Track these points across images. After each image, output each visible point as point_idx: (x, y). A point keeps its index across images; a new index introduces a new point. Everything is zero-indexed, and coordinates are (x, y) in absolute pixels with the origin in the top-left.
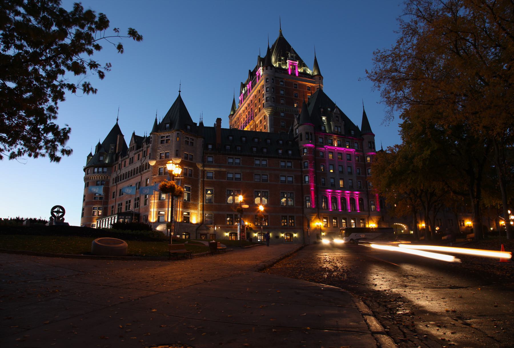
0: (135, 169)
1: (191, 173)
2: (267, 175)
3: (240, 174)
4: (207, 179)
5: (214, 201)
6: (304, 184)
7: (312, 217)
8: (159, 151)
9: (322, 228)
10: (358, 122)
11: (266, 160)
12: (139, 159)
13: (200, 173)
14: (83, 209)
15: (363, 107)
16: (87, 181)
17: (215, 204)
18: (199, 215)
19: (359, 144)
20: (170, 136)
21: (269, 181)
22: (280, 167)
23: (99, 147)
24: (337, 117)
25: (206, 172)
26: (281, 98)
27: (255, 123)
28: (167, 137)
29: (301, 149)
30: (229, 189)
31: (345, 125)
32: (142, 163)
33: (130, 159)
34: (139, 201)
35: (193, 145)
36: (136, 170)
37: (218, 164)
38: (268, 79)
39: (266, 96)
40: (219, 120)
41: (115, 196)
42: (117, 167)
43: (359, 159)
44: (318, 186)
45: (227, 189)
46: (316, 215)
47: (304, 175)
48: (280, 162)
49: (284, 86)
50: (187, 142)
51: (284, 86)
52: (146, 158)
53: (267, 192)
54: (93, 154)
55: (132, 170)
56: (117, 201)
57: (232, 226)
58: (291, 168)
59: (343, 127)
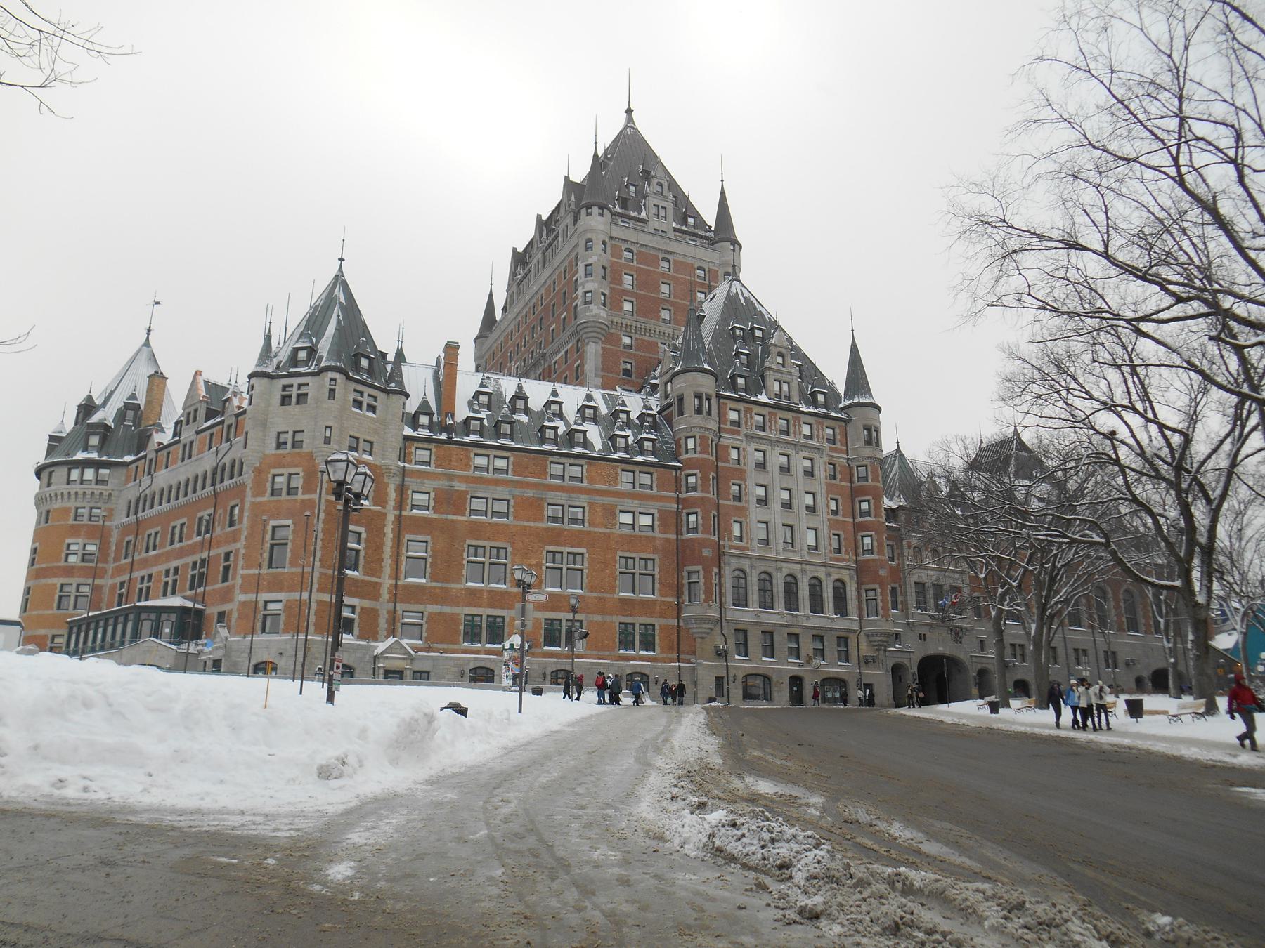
2: (583, 508)
10: (837, 375)
11: (582, 466)
14: (28, 591)
16: (47, 508)
19: (837, 431)
21: (586, 524)
24: (780, 354)
26: (624, 297)
28: (300, 386)
29: (680, 439)
33: (185, 446)
34: (205, 570)
43: (838, 473)
44: (722, 542)
45: (469, 542)
48: (619, 471)
53: (582, 554)
56: (136, 566)
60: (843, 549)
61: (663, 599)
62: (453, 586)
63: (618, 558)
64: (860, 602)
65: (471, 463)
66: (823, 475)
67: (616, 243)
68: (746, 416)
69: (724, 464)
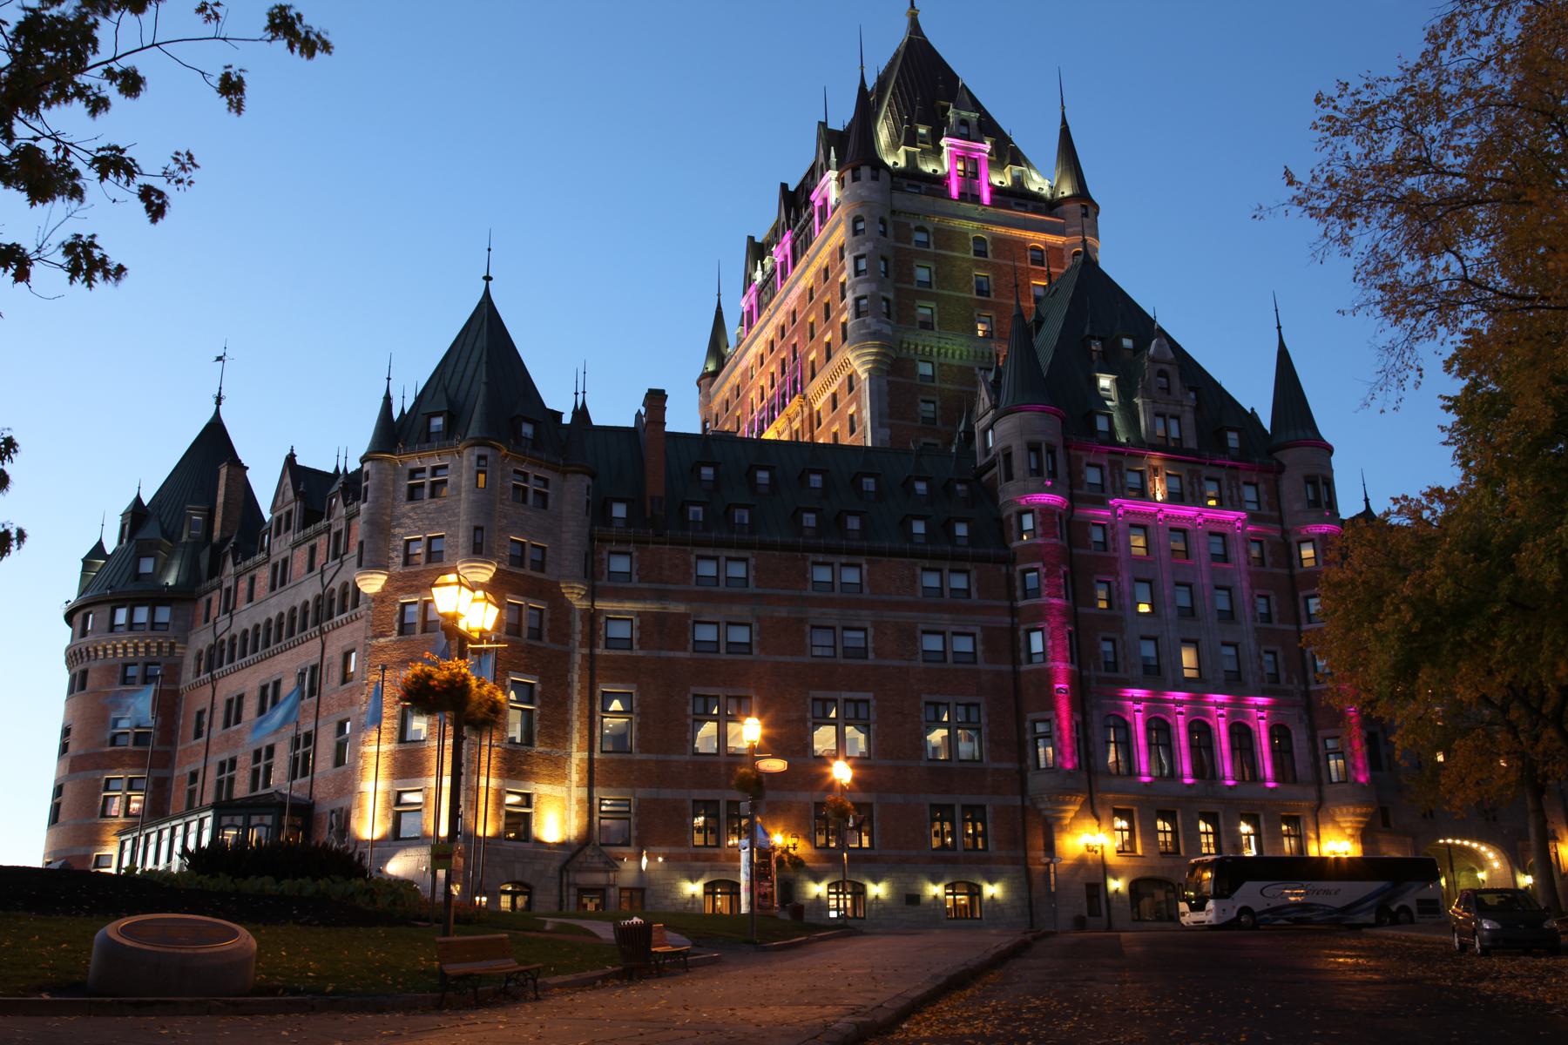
0: (294, 609)
1: (536, 625)
3: (750, 625)
4: (606, 647)
5: (638, 746)
6: (1025, 667)
7: (1065, 811)
8: (402, 531)
9: (1112, 858)
10: (1256, 396)
12: (311, 569)
13: (578, 626)
14: (58, 791)
15: (1279, 328)
16: (81, 667)
17: (644, 756)
18: (575, 807)
19: (1262, 487)
20: (445, 467)
21: (871, 655)
22: (920, 595)
23: (137, 515)
24: (1162, 373)
25: (602, 619)
27: (811, 409)
28: (435, 470)
29: (1009, 517)
30: (701, 691)
31: (1197, 409)
32: (326, 582)
33: (275, 566)
34: (311, 747)
35: (545, 506)
36: (298, 614)
37: (654, 586)
38: (863, 220)
39: (854, 292)
40: (656, 399)
41: (205, 728)
42: (215, 604)
43: (1266, 553)
44: (1085, 673)
45: (693, 690)
46: (1080, 799)
47: (1023, 627)
48: (918, 571)
49: (932, 249)
50: (519, 493)
51: (932, 249)
52: (342, 562)
53: (867, 701)
54: (110, 546)
55: (281, 615)
56: (213, 748)
57: (717, 851)
58: (969, 596)
59: (1189, 418)
60: (1283, 676)
61: (996, 765)
62: (675, 757)
63: (922, 704)
64: (1316, 758)
65: (693, 571)
66: (1242, 558)
67: (902, 219)
68: (1113, 475)
69: (1082, 551)
